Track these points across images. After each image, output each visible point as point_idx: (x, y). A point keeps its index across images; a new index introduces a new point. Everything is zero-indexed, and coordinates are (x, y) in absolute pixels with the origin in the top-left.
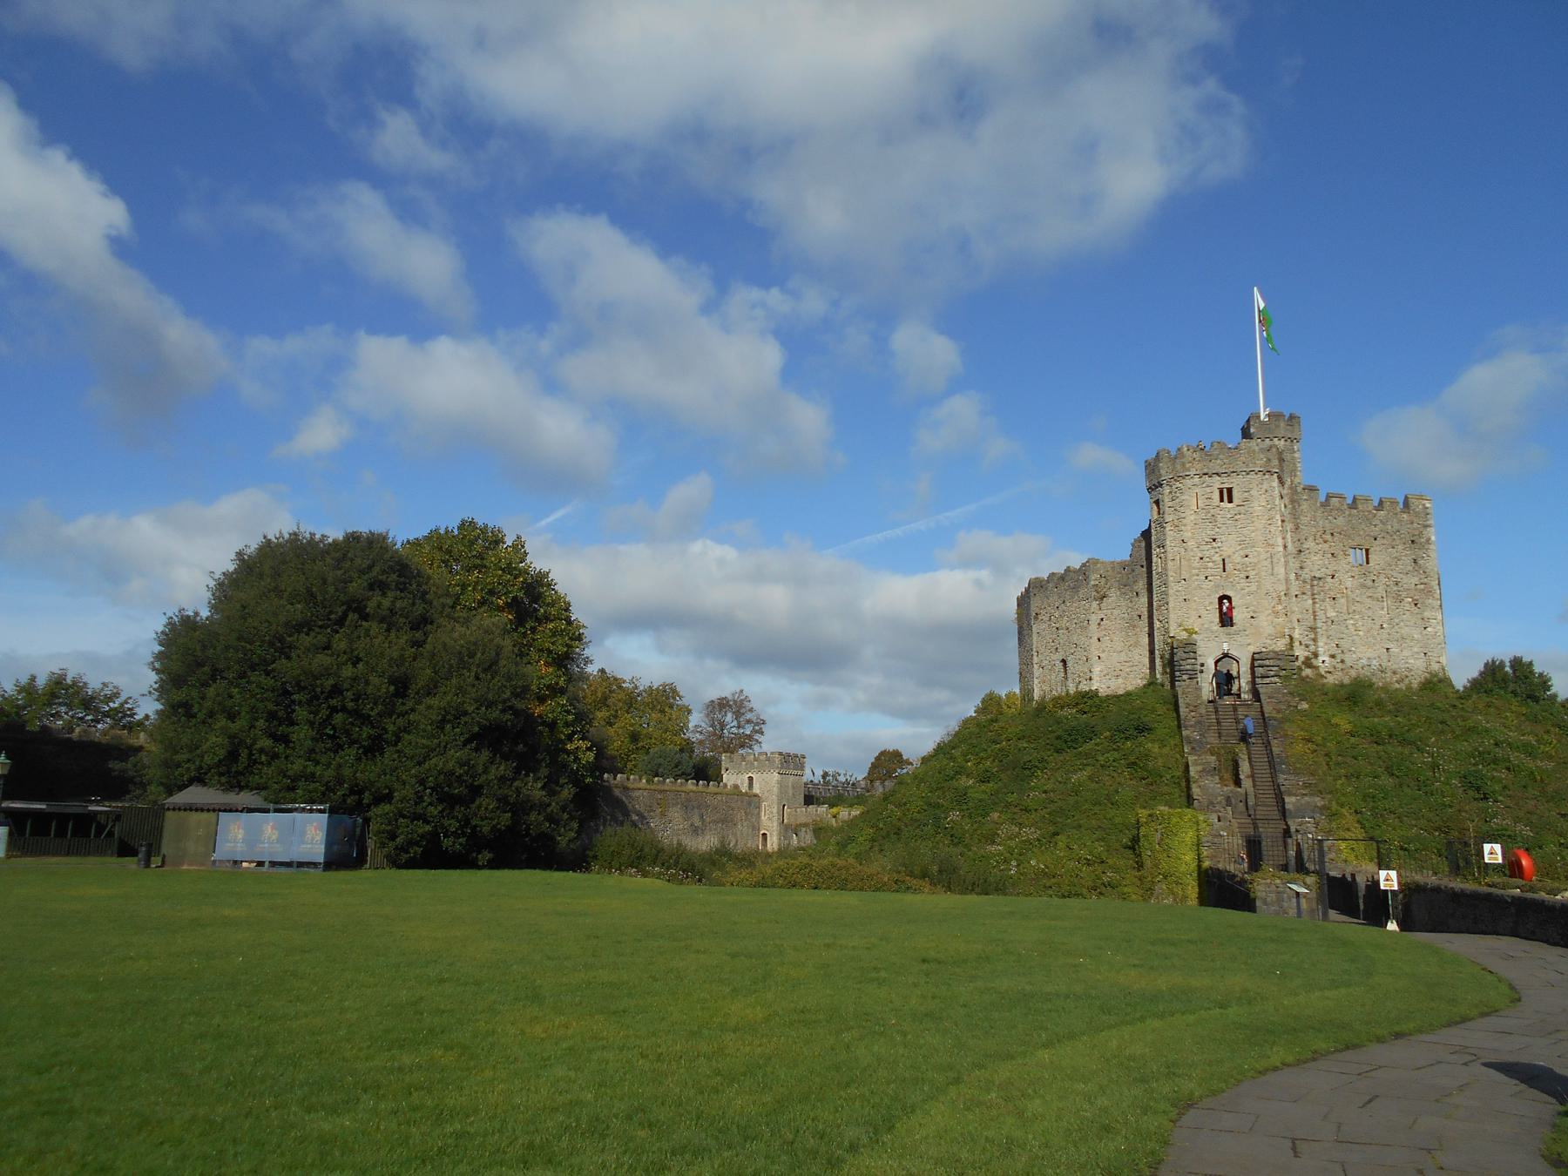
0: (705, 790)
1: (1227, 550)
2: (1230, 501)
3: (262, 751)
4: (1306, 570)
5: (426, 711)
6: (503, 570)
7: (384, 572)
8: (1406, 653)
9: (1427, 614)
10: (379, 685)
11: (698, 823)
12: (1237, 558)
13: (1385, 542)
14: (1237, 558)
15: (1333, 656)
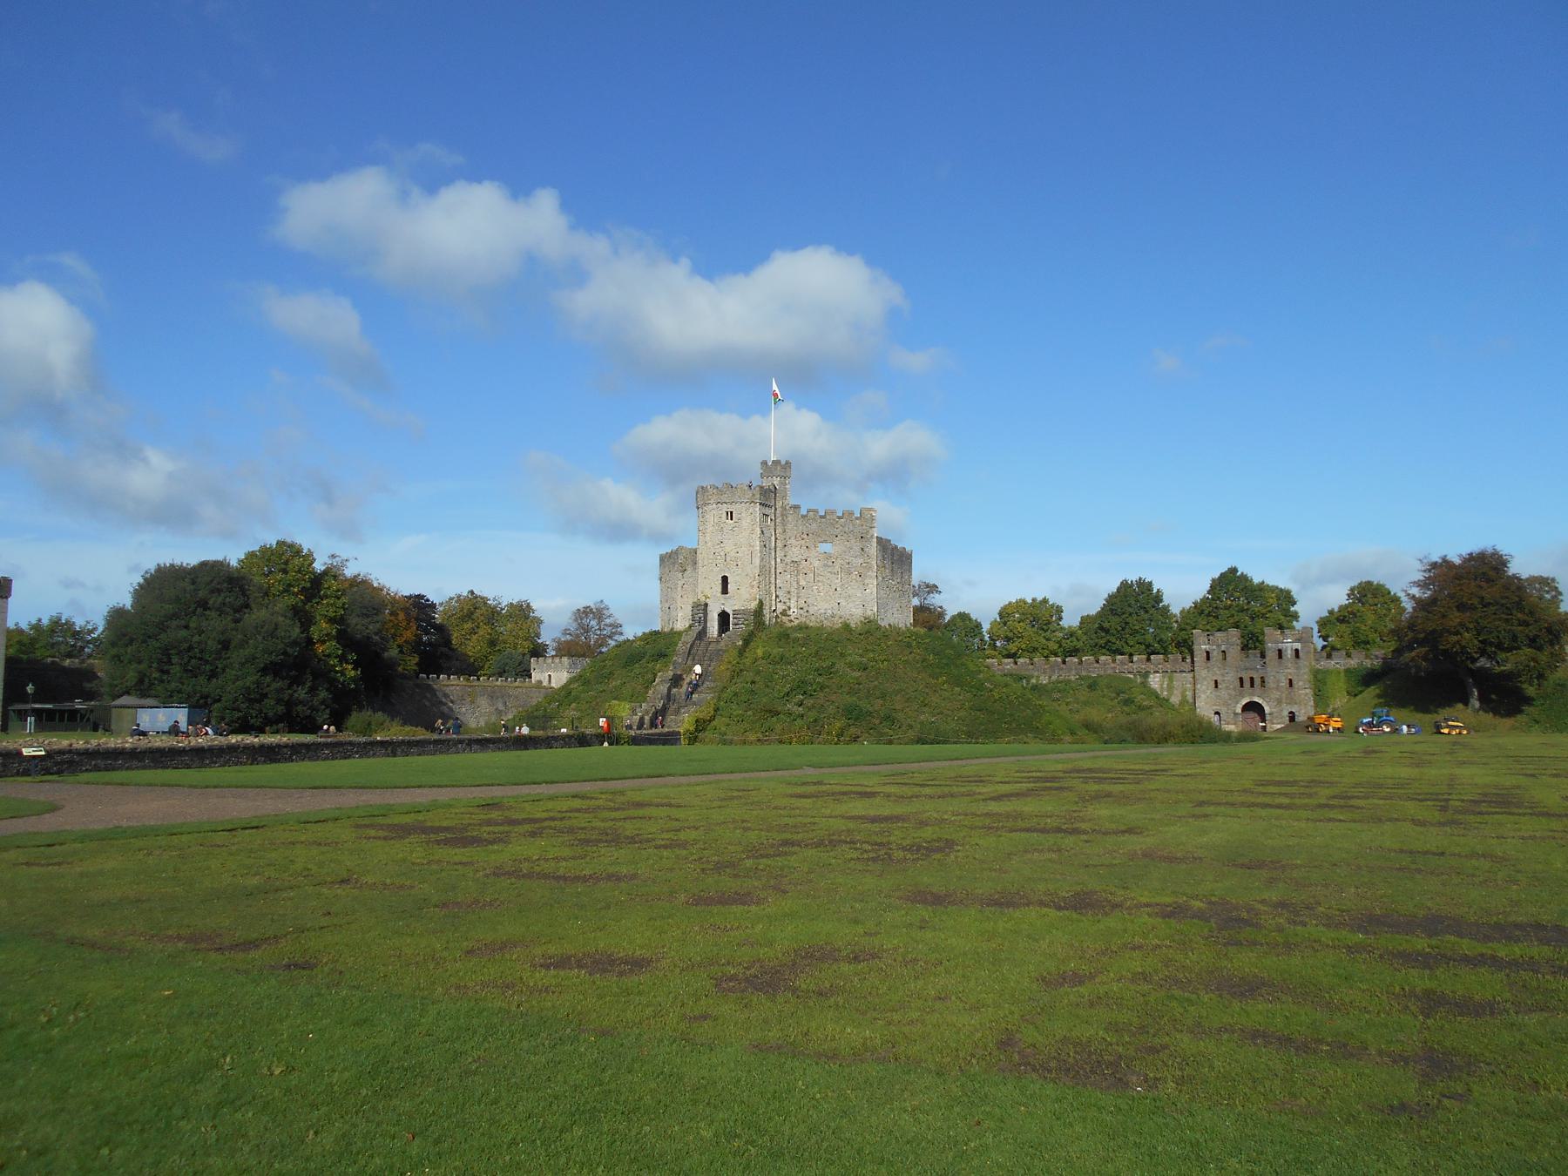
0: (505, 684)
1: (728, 549)
2: (732, 519)
3: (155, 678)
4: (788, 557)
5: (236, 656)
6: (295, 572)
7: (219, 583)
8: (851, 605)
9: (866, 582)
10: (212, 645)
11: (501, 707)
12: (733, 554)
13: (843, 538)
14: (733, 554)
15: (802, 609)
